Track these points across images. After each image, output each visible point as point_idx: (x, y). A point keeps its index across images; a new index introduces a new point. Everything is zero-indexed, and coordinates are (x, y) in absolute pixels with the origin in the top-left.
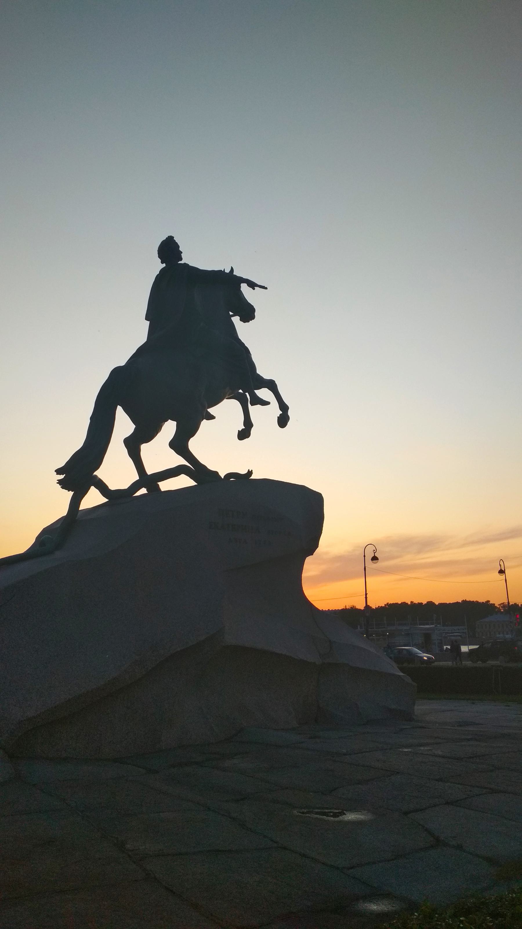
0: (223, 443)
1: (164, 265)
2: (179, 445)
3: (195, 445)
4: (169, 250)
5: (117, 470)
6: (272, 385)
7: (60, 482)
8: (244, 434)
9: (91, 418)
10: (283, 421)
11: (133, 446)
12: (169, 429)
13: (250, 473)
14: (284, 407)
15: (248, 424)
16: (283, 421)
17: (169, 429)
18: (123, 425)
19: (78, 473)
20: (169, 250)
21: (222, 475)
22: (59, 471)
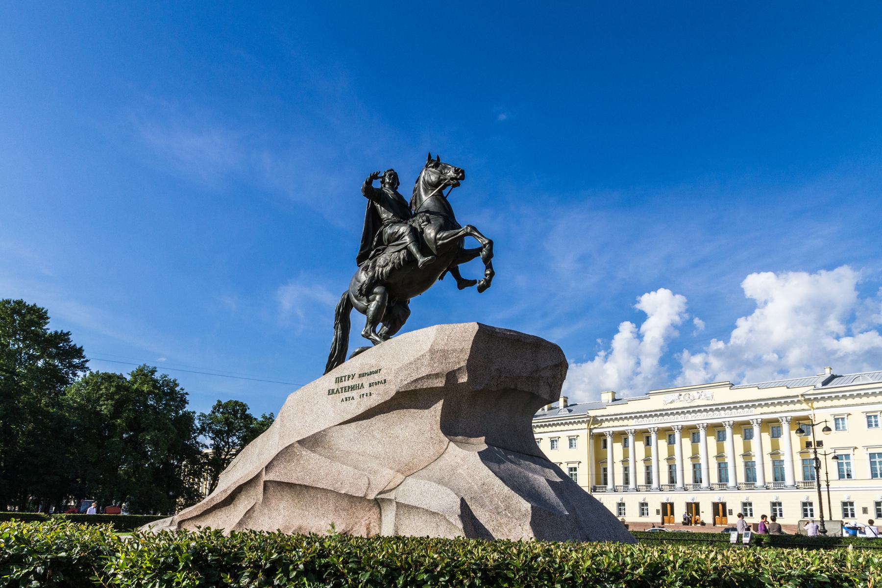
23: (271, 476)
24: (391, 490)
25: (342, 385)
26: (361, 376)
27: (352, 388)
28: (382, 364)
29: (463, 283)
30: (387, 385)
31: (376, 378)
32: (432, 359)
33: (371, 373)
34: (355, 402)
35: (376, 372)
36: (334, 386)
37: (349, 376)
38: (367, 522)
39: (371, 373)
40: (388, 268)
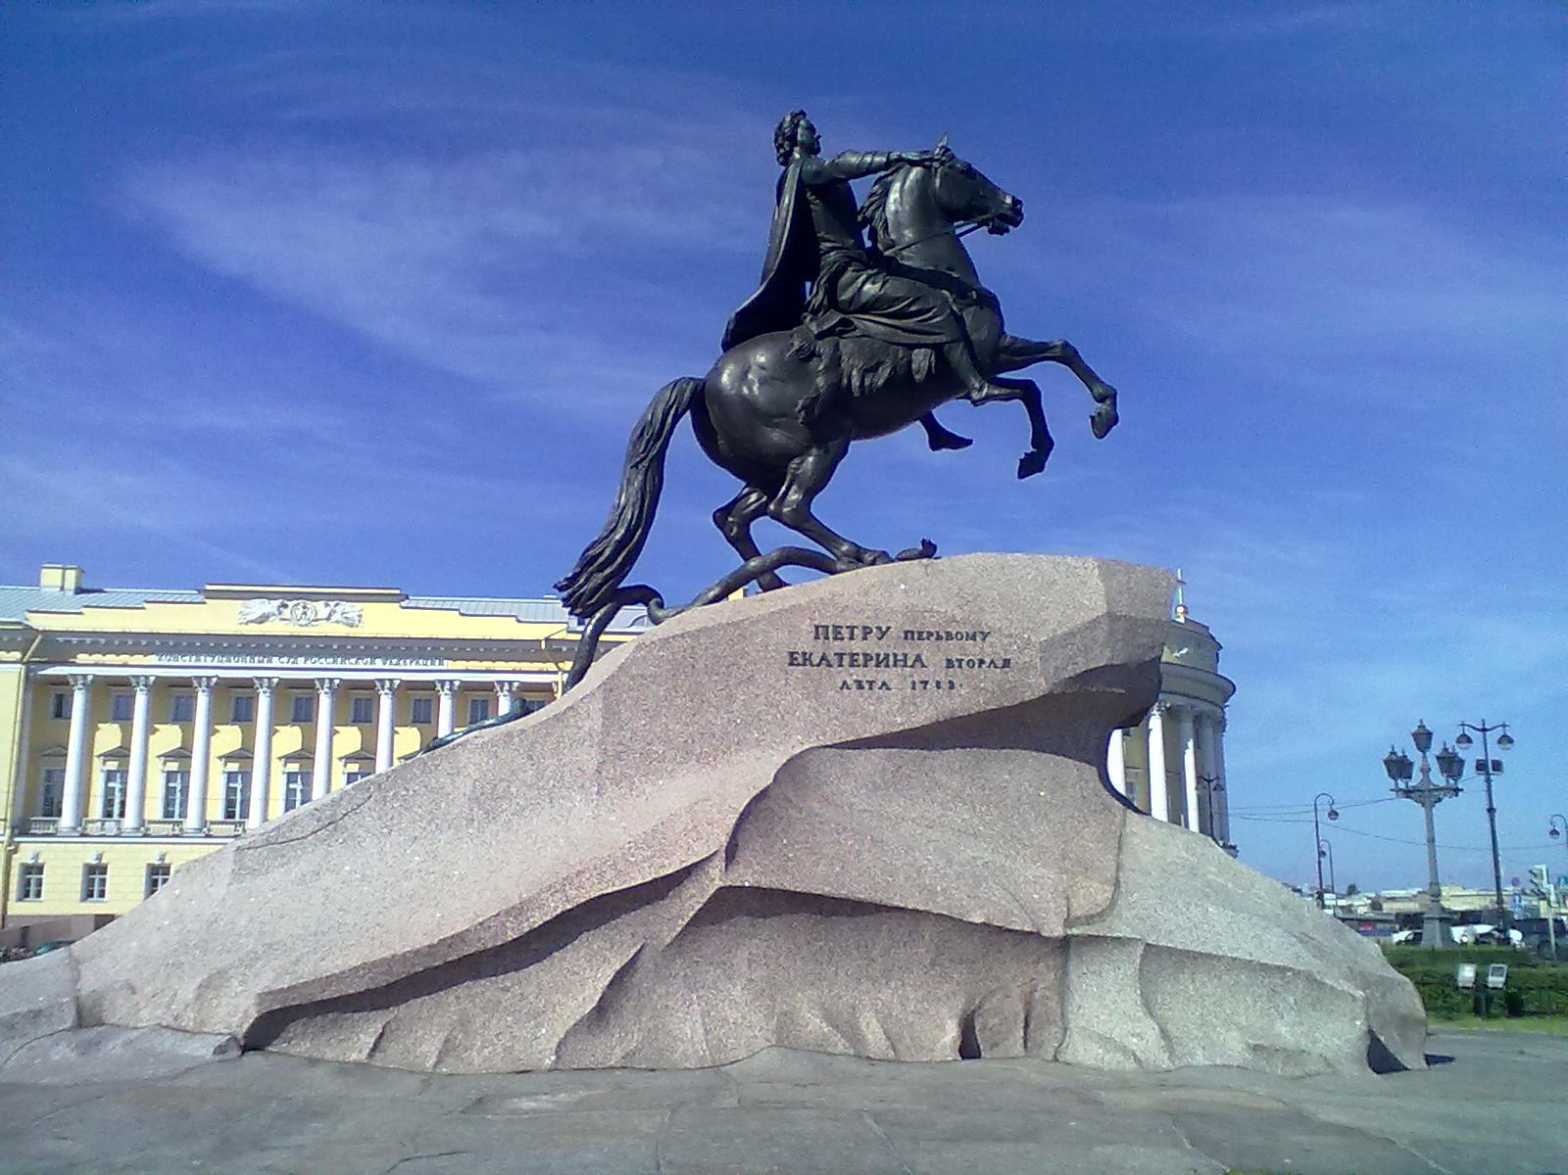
8: (1031, 465)
10: (1103, 425)
14: (1108, 396)
15: (1043, 442)
16: (1103, 425)
23: (746, 876)
24: (1102, 915)
25: (837, 646)
26: (908, 635)
27: (882, 662)
28: (991, 620)
29: (940, 439)
30: (1011, 675)
31: (973, 650)
32: (1112, 633)
33: (949, 636)
34: (893, 698)
35: (974, 638)
36: (817, 650)
37: (867, 631)
38: (1027, 989)
39: (949, 636)
40: (884, 373)
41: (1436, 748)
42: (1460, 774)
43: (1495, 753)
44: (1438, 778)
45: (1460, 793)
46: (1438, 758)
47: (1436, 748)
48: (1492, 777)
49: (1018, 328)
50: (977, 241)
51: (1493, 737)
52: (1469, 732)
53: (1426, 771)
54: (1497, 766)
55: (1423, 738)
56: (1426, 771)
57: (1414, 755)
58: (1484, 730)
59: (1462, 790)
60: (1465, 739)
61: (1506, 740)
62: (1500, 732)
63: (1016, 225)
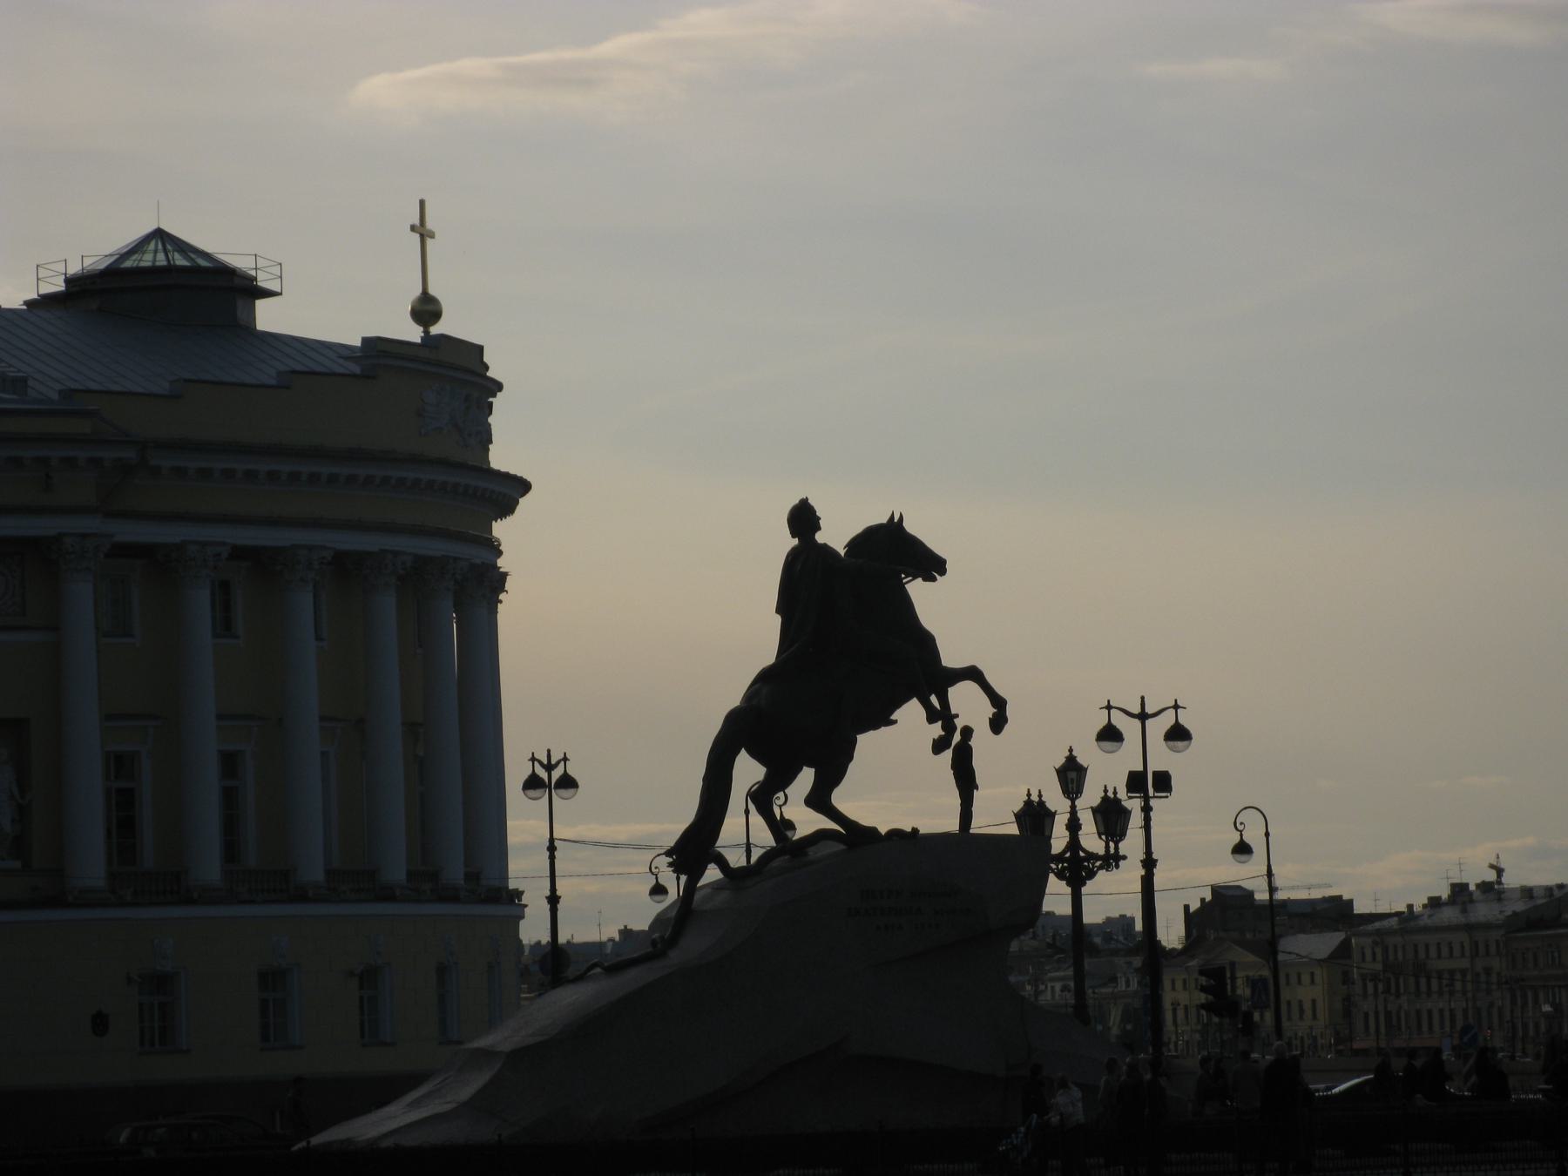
0: (893, 781)
1: (796, 541)
2: (819, 800)
3: (841, 799)
4: (803, 519)
5: (743, 835)
6: (973, 674)
7: (670, 865)
9: (704, 779)
11: (762, 798)
12: (806, 778)
13: (915, 831)
17: (806, 778)
18: (747, 771)
19: (694, 849)
20: (803, 519)
21: (883, 830)
22: (668, 853)
41: (1091, 796)
42: (1122, 835)
43: (1162, 758)
44: (1092, 841)
45: (1122, 863)
46: (1095, 811)
47: (1091, 796)
48: (1152, 802)
49: (951, 658)
50: (917, 589)
51: (1159, 727)
52: (1119, 721)
53: (1074, 825)
54: (1163, 782)
55: (1071, 775)
56: (1074, 825)
57: (1056, 801)
58: (1143, 716)
59: (1124, 858)
60: (1110, 735)
61: (1178, 734)
62: (1167, 720)
63: (943, 572)
